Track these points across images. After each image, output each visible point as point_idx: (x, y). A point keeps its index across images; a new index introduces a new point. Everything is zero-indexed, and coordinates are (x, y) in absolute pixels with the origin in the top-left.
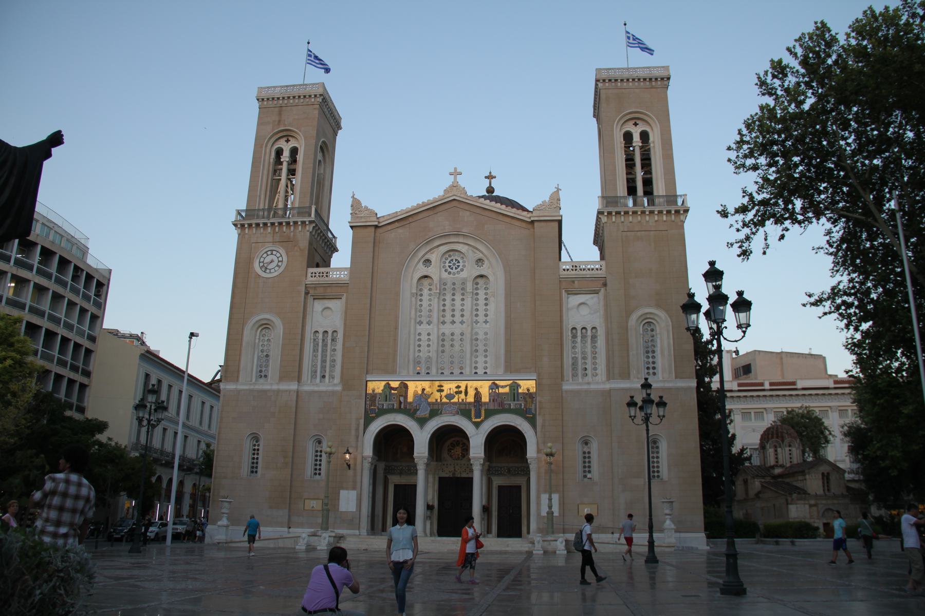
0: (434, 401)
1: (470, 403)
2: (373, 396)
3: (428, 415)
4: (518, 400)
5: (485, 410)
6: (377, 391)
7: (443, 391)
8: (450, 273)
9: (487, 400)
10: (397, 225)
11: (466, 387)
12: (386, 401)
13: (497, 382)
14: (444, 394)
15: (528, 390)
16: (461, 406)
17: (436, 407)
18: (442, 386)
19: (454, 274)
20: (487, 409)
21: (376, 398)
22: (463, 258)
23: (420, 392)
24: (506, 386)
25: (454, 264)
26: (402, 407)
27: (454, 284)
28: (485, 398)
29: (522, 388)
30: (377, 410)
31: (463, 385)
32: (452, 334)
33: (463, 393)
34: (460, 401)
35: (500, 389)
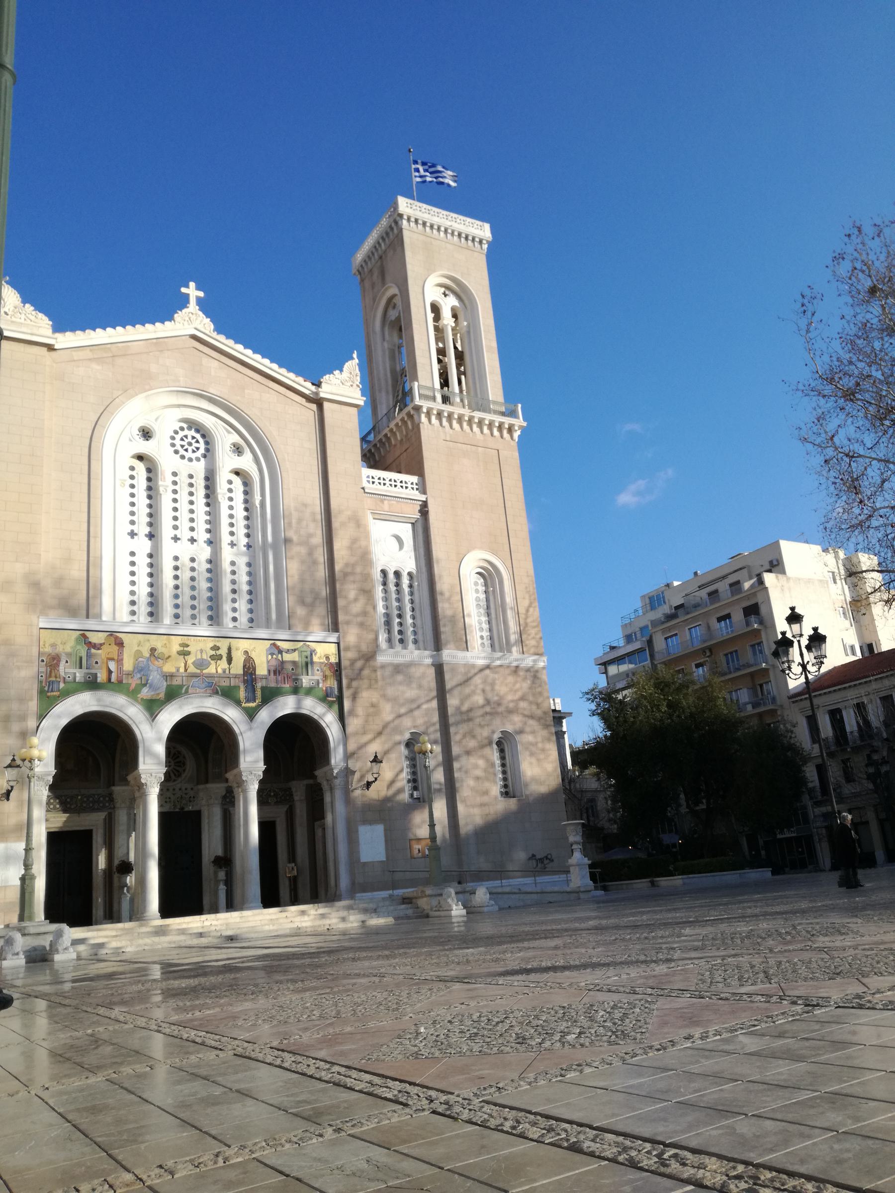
0: (173, 670)
1: (236, 676)
2: (54, 659)
3: (162, 696)
4: (313, 675)
5: (263, 688)
6: (60, 649)
7: (189, 653)
8: (183, 457)
9: (265, 672)
10: (87, 354)
11: (229, 649)
12: (81, 667)
13: (278, 643)
14: (191, 660)
15: (327, 658)
16: (222, 680)
17: (177, 682)
18: (188, 646)
19: (190, 460)
20: (266, 687)
21: (59, 661)
22: (203, 436)
23: (147, 654)
24: (294, 650)
25: (190, 444)
26: (113, 680)
27: (191, 476)
28: (262, 670)
29: (318, 655)
30: (62, 685)
31: (223, 645)
32: (193, 560)
33: (224, 658)
34: (220, 671)
35: (284, 653)
